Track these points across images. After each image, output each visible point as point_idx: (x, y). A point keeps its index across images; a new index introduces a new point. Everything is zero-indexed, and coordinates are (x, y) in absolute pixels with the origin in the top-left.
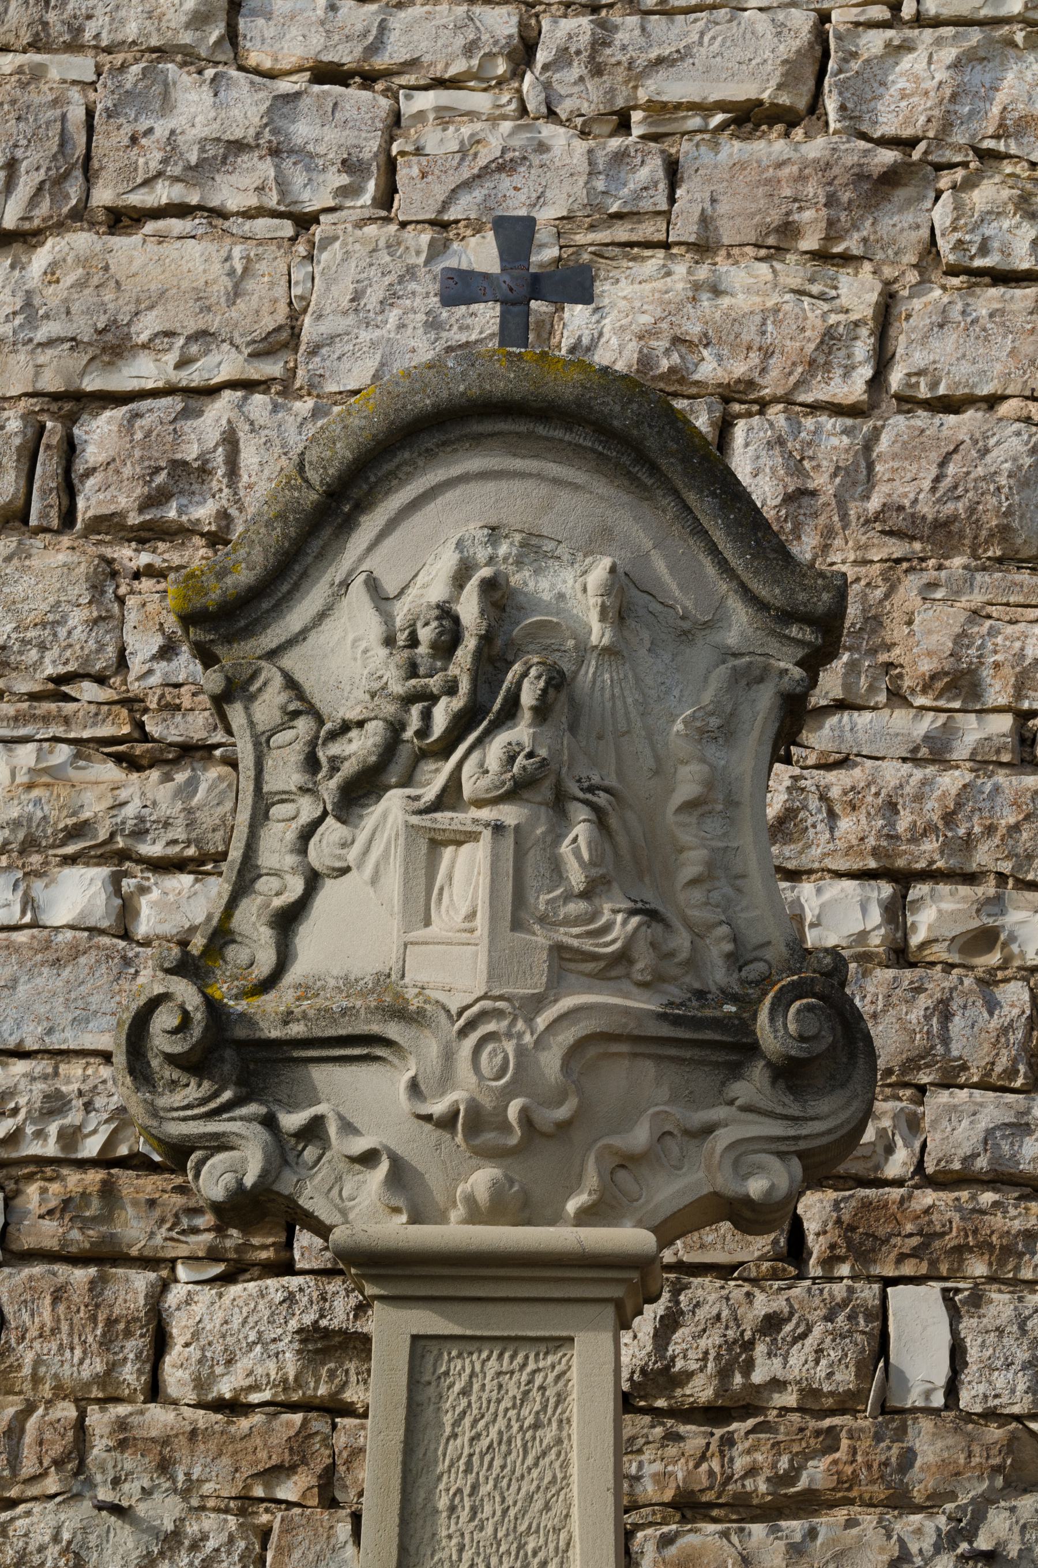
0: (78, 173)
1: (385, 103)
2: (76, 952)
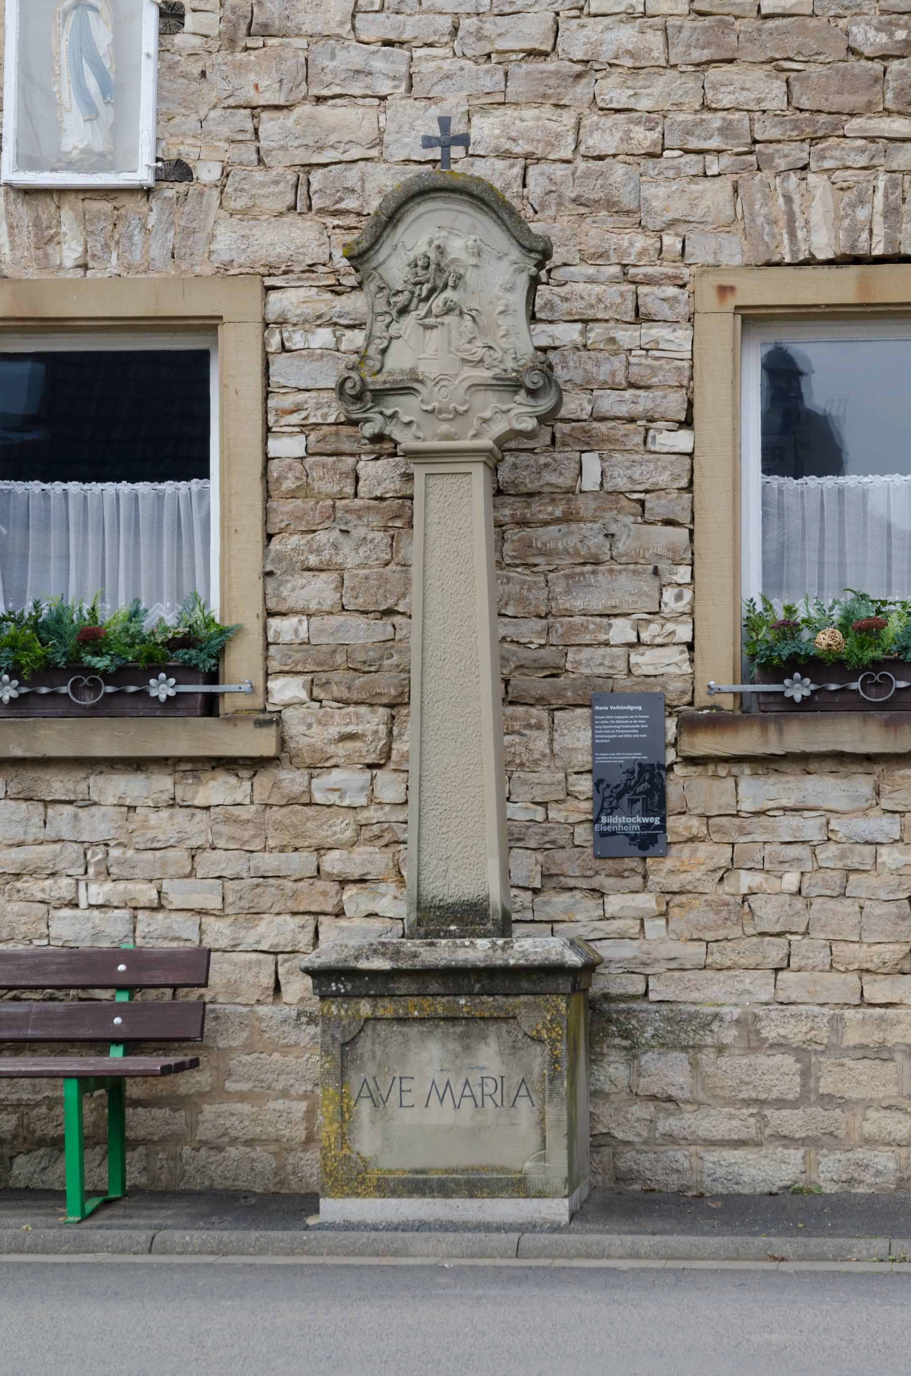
0: (304, 83)
1: (407, 53)
2: (322, 356)
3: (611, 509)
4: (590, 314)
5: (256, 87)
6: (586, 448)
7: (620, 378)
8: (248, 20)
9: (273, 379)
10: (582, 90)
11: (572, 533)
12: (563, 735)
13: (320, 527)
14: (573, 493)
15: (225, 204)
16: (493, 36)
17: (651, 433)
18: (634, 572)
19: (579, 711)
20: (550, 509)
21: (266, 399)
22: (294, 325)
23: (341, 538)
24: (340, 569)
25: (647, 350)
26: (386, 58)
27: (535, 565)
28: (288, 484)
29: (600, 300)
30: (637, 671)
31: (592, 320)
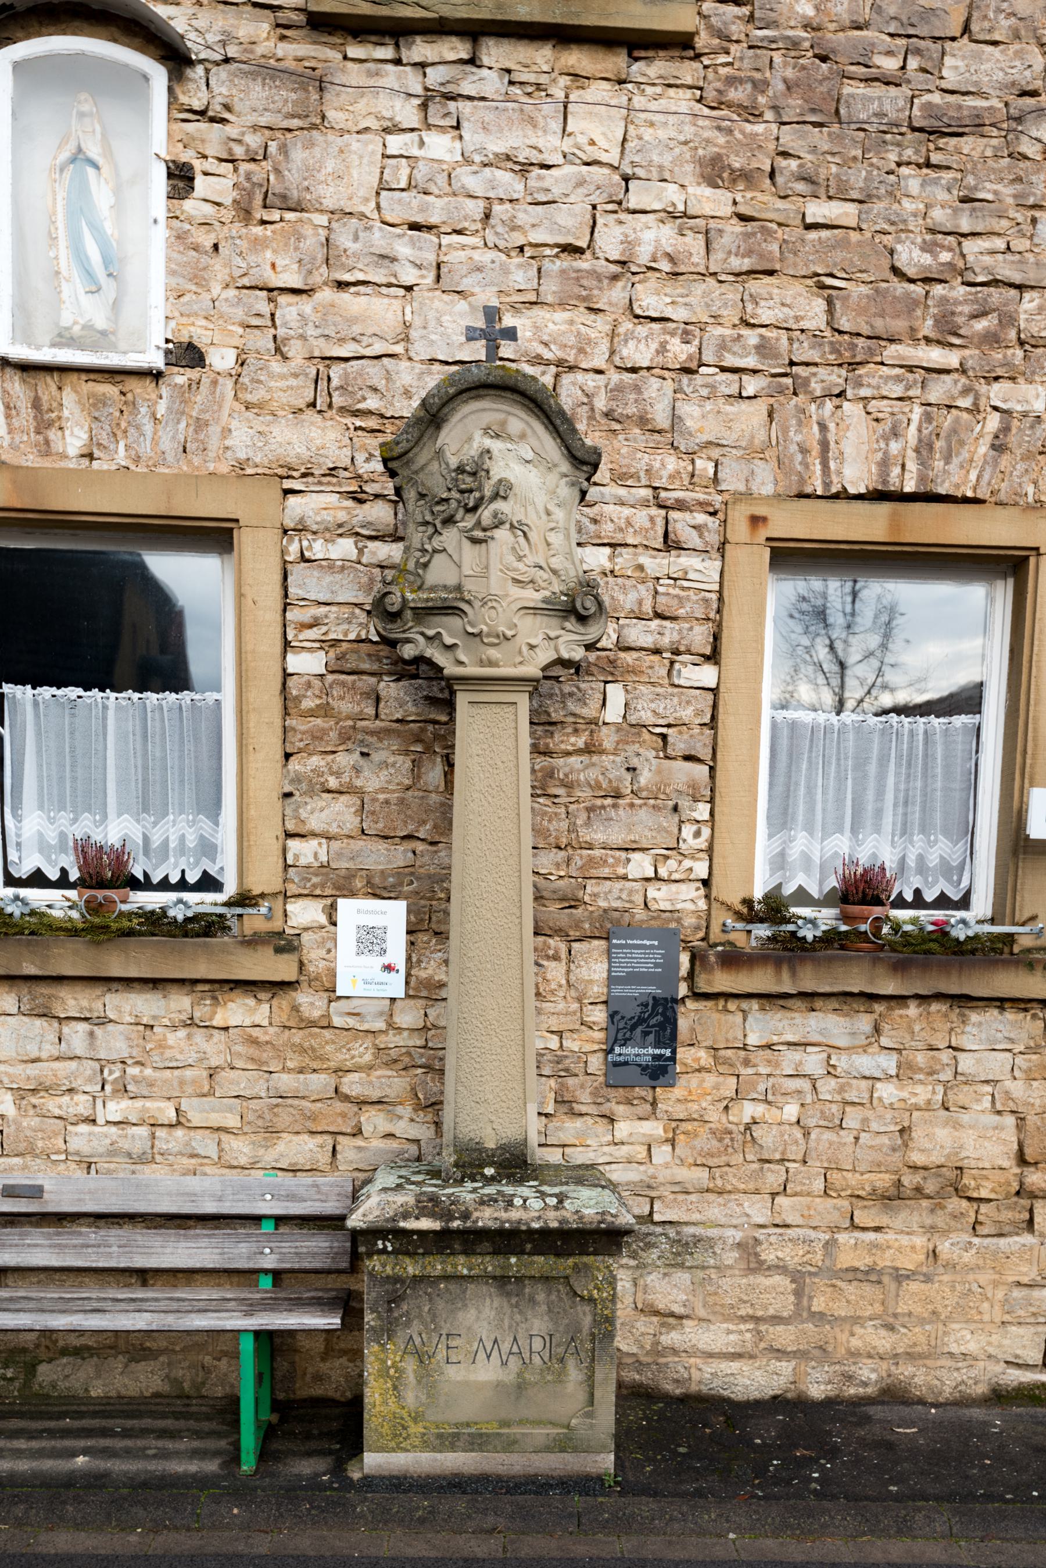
1: (436, 240)
2: (343, 568)
5: (273, 265)
8: (264, 190)
9: (291, 590)
10: (618, 293)
12: (580, 966)
13: (341, 748)
15: (240, 395)
16: (527, 227)
21: (285, 611)
22: (314, 533)
23: (362, 761)
24: (359, 792)
26: (412, 242)
28: (308, 704)
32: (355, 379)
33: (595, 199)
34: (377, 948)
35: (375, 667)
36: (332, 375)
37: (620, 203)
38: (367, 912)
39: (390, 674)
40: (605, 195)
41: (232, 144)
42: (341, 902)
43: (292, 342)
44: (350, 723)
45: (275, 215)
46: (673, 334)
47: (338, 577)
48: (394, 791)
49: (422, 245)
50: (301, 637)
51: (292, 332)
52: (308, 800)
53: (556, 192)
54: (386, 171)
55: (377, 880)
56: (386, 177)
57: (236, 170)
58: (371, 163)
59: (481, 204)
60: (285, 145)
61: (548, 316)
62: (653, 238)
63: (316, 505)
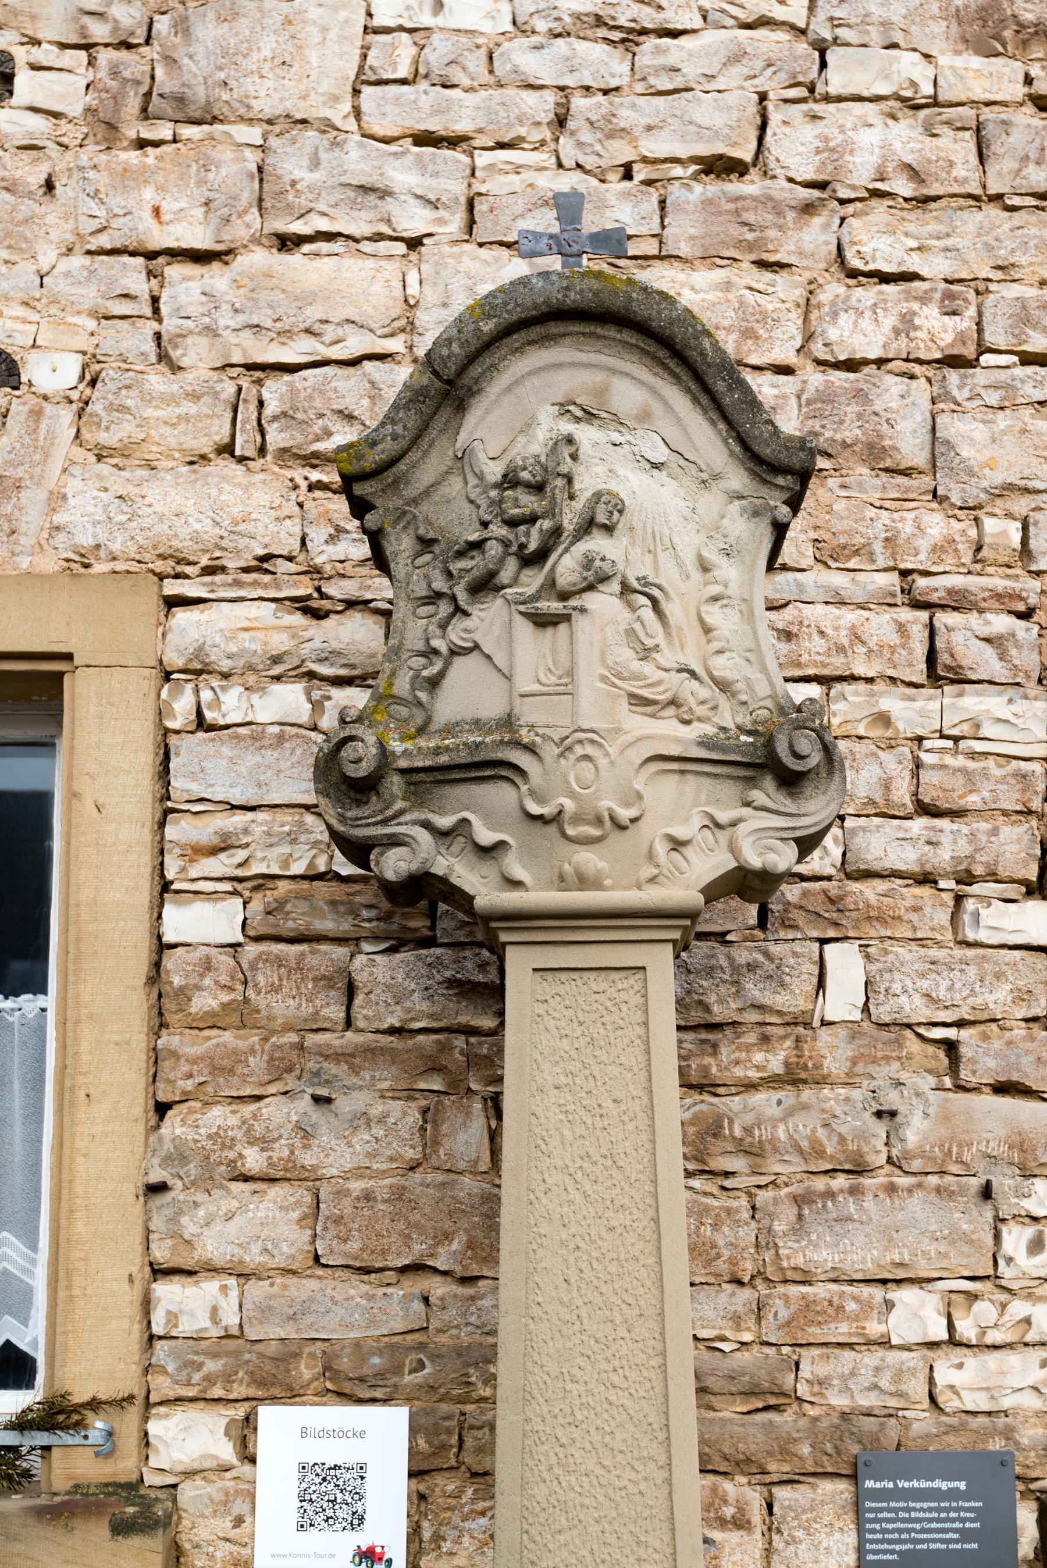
0: (255, 210)
1: (465, 159)
2: (281, 738)
3: (887, 1059)
4: (837, 665)
5: (157, 211)
6: (831, 933)
7: (902, 794)
8: (144, 89)
9: (178, 783)
10: (815, 237)
11: (805, 1107)
12: (793, 1541)
13: (272, 1089)
14: (807, 1025)
15: (86, 435)
16: (637, 131)
17: (970, 905)
18: (938, 1190)
19: (827, 1486)
20: (759, 1057)
21: (162, 825)
22: (226, 676)
23: (316, 1115)
24: (310, 1178)
25: (956, 739)
26: (421, 165)
27: (727, 1174)
28: (204, 1002)
29: (857, 637)
30: (949, 1402)
31: (841, 679)
32: (310, 398)
33: (762, 83)
34: (343, 1512)
35: (345, 926)
36: (266, 395)
37: (812, 90)
38: (324, 1434)
39: (375, 938)
40: (782, 76)
41: (87, 20)
42: (266, 1414)
43: (190, 340)
44: (293, 1038)
45: (164, 131)
46: (924, 299)
47: (271, 755)
48: (383, 1174)
49: (440, 167)
50: (193, 873)
51: (189, 324)
52: (200, 1197)
53: (691, 72)
54: (371, 54)
55: (345, 1363)
56: (370, 60)
57: (91, 63)
58: (343, 38)
59: (550, 98)
60: (185, 19)
61: (681, 277)
62: (874, 144)
63: (232, 624)
